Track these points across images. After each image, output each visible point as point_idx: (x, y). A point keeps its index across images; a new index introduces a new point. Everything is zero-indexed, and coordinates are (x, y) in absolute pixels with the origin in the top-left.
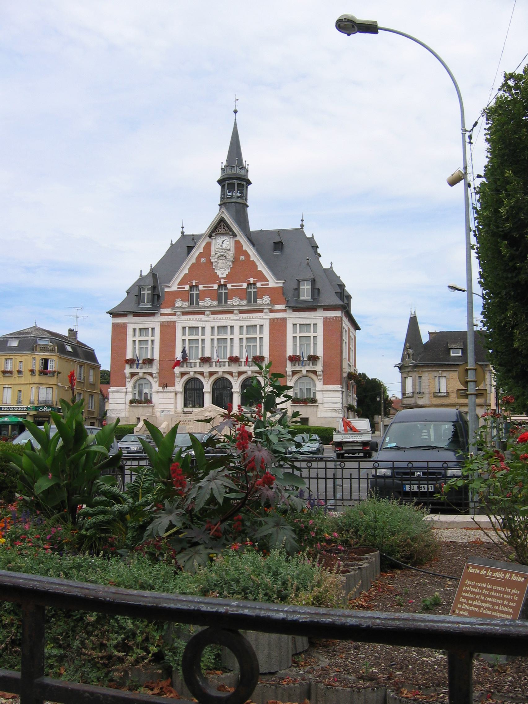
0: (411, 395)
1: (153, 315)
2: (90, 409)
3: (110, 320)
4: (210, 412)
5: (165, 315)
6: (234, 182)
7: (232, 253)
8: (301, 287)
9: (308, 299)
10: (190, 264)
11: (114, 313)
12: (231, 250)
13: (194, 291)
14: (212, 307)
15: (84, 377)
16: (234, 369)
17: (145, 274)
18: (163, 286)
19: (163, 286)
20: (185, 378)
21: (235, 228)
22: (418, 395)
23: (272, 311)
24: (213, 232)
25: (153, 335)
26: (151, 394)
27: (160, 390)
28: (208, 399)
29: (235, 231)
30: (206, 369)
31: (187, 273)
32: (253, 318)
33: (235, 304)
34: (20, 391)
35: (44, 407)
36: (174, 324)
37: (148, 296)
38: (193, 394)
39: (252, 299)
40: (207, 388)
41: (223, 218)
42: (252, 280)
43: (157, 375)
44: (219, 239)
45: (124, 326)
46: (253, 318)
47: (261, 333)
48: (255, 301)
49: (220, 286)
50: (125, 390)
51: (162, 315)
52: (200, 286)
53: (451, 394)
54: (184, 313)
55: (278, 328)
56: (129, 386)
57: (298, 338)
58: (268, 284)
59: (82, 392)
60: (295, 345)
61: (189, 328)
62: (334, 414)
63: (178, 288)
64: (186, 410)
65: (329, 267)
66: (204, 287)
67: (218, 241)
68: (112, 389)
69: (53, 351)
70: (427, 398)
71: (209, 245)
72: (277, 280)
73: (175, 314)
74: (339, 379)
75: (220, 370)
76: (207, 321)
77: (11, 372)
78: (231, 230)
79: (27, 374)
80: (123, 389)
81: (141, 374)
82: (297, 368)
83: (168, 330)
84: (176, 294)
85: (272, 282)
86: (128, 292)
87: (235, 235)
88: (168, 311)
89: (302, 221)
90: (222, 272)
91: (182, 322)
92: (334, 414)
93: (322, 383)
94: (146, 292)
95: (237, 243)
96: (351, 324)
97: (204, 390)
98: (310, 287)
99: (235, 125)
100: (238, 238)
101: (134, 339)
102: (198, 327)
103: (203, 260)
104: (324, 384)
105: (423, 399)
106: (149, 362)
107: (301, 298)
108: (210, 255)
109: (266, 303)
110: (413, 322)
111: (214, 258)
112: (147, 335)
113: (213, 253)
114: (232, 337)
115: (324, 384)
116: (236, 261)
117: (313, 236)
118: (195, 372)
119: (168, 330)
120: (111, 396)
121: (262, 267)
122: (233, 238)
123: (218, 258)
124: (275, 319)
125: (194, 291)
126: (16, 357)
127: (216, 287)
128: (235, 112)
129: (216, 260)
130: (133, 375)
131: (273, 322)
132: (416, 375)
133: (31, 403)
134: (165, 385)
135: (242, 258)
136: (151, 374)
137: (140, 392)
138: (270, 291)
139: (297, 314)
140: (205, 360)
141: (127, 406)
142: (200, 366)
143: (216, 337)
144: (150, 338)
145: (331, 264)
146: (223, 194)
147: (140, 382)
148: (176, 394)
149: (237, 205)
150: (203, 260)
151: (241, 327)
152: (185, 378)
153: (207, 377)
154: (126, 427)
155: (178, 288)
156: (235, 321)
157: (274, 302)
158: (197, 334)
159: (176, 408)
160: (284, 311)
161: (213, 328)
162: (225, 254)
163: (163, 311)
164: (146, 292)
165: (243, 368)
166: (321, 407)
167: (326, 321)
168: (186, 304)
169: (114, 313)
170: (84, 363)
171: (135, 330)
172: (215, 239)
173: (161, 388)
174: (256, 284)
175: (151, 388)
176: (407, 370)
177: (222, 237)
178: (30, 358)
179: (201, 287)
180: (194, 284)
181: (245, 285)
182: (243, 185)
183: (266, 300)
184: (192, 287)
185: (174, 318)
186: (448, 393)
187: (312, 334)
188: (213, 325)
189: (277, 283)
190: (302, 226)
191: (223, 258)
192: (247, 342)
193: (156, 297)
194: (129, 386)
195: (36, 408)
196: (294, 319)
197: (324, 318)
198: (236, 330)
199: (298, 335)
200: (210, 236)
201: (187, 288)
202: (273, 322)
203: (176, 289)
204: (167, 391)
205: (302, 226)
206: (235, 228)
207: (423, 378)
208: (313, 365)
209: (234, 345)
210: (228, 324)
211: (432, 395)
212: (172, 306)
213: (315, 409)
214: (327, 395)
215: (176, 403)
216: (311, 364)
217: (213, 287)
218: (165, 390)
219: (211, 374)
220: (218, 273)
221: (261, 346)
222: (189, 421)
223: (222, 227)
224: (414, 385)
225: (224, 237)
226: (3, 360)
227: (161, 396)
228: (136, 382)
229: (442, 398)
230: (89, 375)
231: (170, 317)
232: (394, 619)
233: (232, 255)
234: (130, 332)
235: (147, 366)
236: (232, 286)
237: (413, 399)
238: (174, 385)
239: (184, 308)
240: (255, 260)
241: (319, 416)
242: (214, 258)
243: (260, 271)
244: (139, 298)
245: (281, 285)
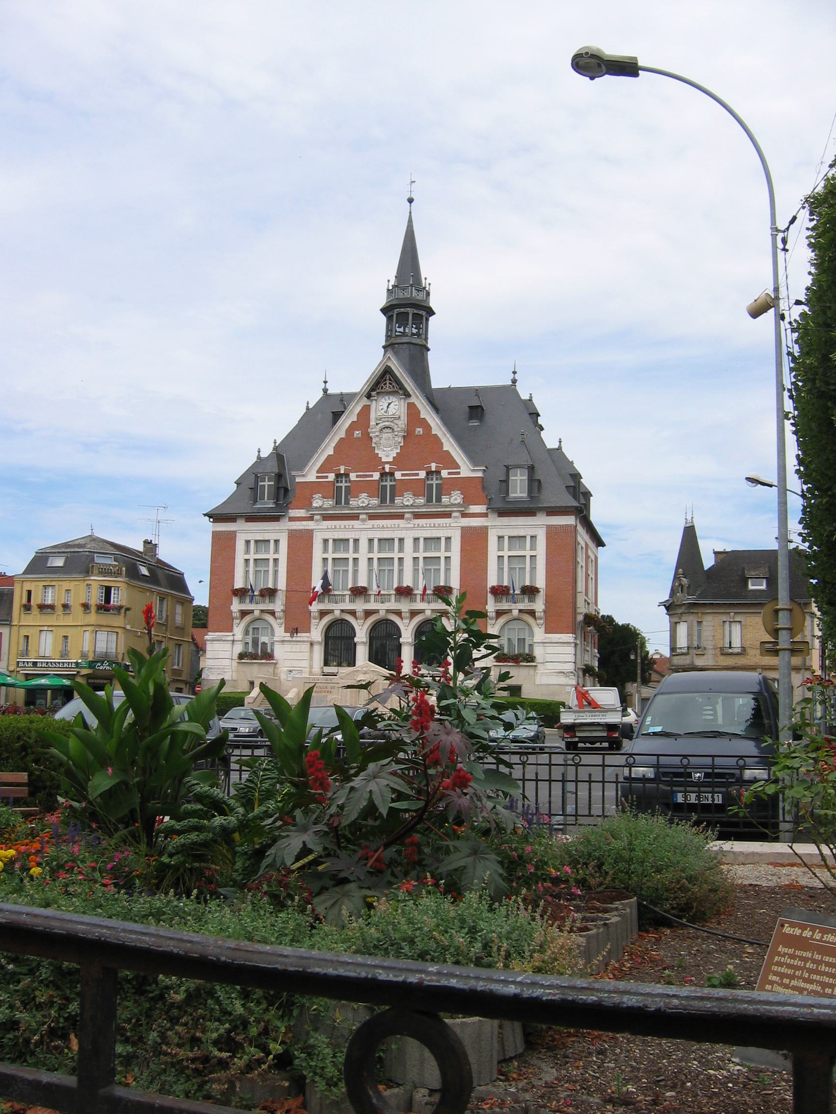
0: (685, 651)
1: (277, 519)
2: (176, 667)
3: (209, 527)
4: (365, 673)
5: (298, 519)
6: (408, 311)
7: (402, 423)
8: (512, 478)
9: (522, 497)
10: (336, 439)
11: (216, 516)
12: (402, 418)
13: (341, 482)
14: (370, 508)
15: (167, 616)
16: (405, 606)
17: (265, 454)
18: (293, 473)
19: (293, 473)
20: (327, 619)
21: (409, 384)
22: (695, 651)
23: (464, 515)
24: (373, 389)
25: (276, 551)
26: (272, 644)
27: (286, 639)
28: (362, 653)
29: (409, 389)
30: (360, 606)
32: (434, 526)
34: (66, 637)
35: (103, 662)
36: (309, 533)
37: (270, 489)
38: (338, 646)
39: (433, 497)
40: (361, 635)
41: (389, 367)
42: (433, 467)
43: (281, 614)
44: (383, 400)
45: (231, 537)
46: (434, 526)
47: (448, 549)
48: (439, 500)
49: (383, 474)
50: (231, 638)
51: (292, 519)
52: (351, 475)
53: (748, 650)
54: (326, 518)
55: (474, 542)
56: (238, 631)
57: (506, 559)
58: (459, 473)
59: (163, 639)
60: (500, 569)
61: (334, 540)
62: (562, 680)
63: (318, 477)
64: (327, 669)
65: (555, 445)
66: (357, 476)
67: (381, 404)
68: (210, 636)
69: (118, 574)
70: (710, 657)
71: (366, 410)
72: (475, 466)
73: (311, 518)
74: (570, 625)
75: (382, 607)
76: (362, 530)
77: (52, 607)
78: (401, 387)
79: (77, 609)
80: (228, 636)
81: (257, 613)
82: (505, 606)
83: (300, 544)
84: (314, 487)
85: (466, 470)
86: (238, 483)
87: (408, 395)
88: (301, 513)
89: (514, 373)
90: (387, 453)
91: (323, 531)
92: (562, 680)
93: (543, 629)
94: (266, 483)
95: (412, 407)
96: (591, 538)
97: (356, 640)
98: (526, 478)
99: (410, 221)
100: (413, 400)
101: (247, 557)
102: (348, 540)
103: (357, 434)
104: (547, 632)
105: (704, 657)
106: (270, 593)
107: (512, 495)
109: (456, 502)
110: (690, 536)
111: (374, 431)
112: (267, 551)
113: (373, 423)
114: (401, 555)
115: (547, 632)
116: (408, 435)
117: (531, 397)
118: (342, 611)
119: (300, 544)
120: (209, 647)
121: (449, 445)
122: (405, 399)
124: (470, 528)
125: (341, 482)
126: (60, 583)
127: (376, 476)
128: (411, 201)
129: (377, 434)
130: (244, 613)
132: (693, 619)
133: (84, 655)
134: (294, 631)
135: (419, 431)
136: (272, 613)
137: (255, 642)
138: (463, 484)
139: (505, 520)
140: (359, 592)
141: (235, 663)
142: (350, 601)
143: (376, 555)
144: (271, 556)
145: (560, 442)
146: (389, 329)
147: (256, 625)
148: (312, 644)
149: (412, 347)
150: (357, 434)
151: (416, 540)
152: (327, 619)
153: (360, 619)
154: (233, 695)
155: (318, 477)
156: (406, 530)
157: (468, 500)
158: (347, 550)
159: (311, 667)
160: (485, 515)
161: (371, 541)
163: (293, 513)
164: (266, 483)
165: (419, 605)
166: (541, 669)
167: (552, 533)
168: (330, 503)
169: (216, 516)
170: (168, 594)
171: (248, 542)
172: (376, 400)
173: (288, 634)
174: (440, 472)
175: (273, 634)
176: (679, 611)
177: (387, 398)
178: (82, 586)
179: (353, 476)
180: (342, 472)
181: (422, 474)
182: (422, 316)
183: (457, 497)
184: (338, 476)
185: (310, 525)
186: (743, 648)
187: (528, 553)
188: (371, 537)
189: (473, 470)
190: (514, 381)
192: (425, 564)
193: (282, 491)
194: (238, 631)
195: (92, 664)
196: (499, 528)
197: (549, 527)
198: (409, 544)
199: (506, 553)
201: (331, 477)
203: (314, 480)
204: (298, 639)
205: (514, 381)
206: (409, 384)
207: (704, 623)
208: (530, 601)
209: (405, 568)
210: (396, 535)
211: (718, 652)
212: (308, 506)
213: (531, 671)
214: (550, 649)
215: (311, 659)
216: (526, 600)
217: (372, 476)
218: (294, 639)
219: (368, 613)
220: (381, 454)
221: (447, 570)
222: (332, 687)
223: (388, 382)
224: (690, 635)
225: (391, 397)
226: (41, 587)
227: (287, 647)
228: (248, 626)
229: (734, 657)
230: (174, 614)
231: (304, 523)
232: (701, 998)
233: (403, 426)
234: (240, 546)
235: (267, 600)
236: (403, 475)
237: (688, 657)
238: (309, 631)
239: (326, 509)
240: (440, 434)
241: (538, 682)
242: (374, 430)
243: (447, 452)
244: (255, 492)
245: (480, 474)
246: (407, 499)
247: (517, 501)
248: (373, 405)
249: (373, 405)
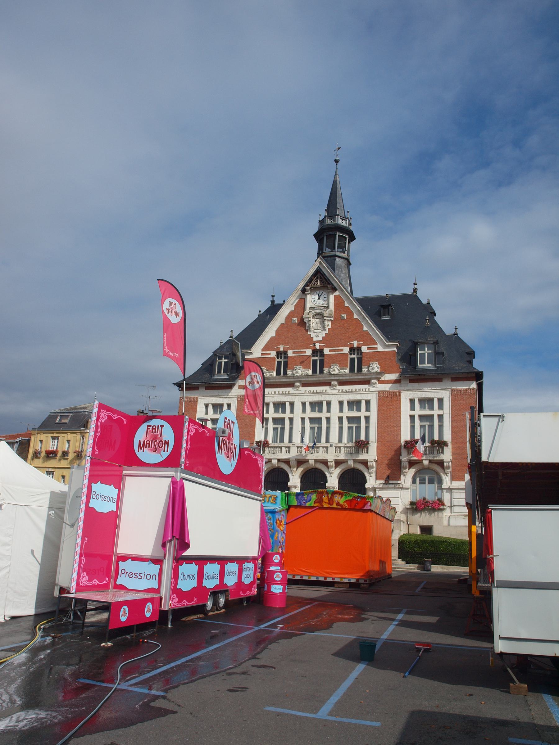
9: (429, 367)
31: (274, 335)
33: (333, 373)
49: (315, 352)
55: (389, 404)
58: (376, 348)
63: (262, 354)
66: (294, 353)
71: (302, 301)
72: (390, 342)
78: (329, 283)
104: (453, 479)
109: (374, 371)
115: (453, 479)
126: (63, 435)
127: (309, 352)
131: (382, 396)
155: (262, 354)
156: (334, 395)
161: (304, 404)
164: (223, 360)
179: (290, 353)
181: (346, 350)
191: (321, 317)
201: (273, 354)
202: (382, 396)
217: (305, 352)
220: (312, 335)
236: (330, 351)
242: (308, 316)
246: (336, 370)
247: (424, 371)
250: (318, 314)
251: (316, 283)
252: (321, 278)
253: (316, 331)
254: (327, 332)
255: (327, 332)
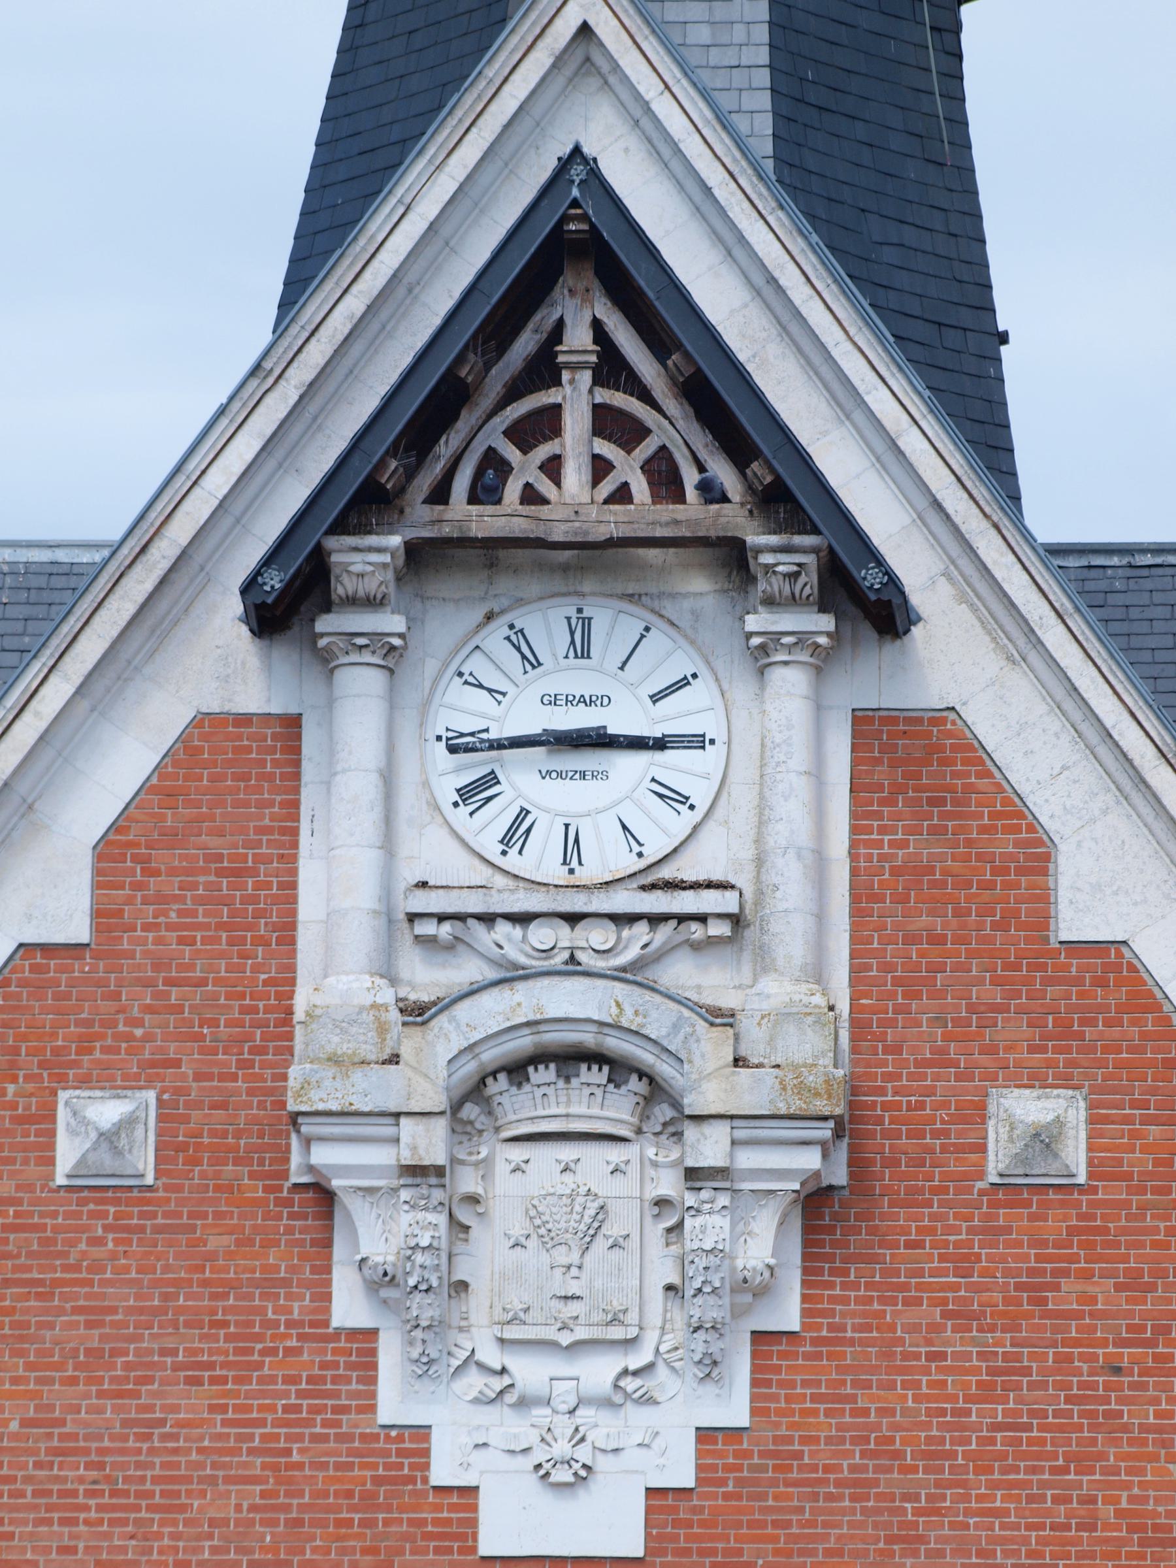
7: (790, 1000)
12: (788, 928)
24: (359, 497)
71: (240, 782)
87: (868, 605)
95: (914, 771)
108: (277, 1027)
122: (824, 661)
123: (470, 1102)
162: (659, 1019)
172: (391, 655)
177: (547, 626)
191: (616, 1108)
200: (291, 601)
223: (576, 398)
242: (371, 1089)
248: (354, 724)
249: (354, 724)
250: (570, 1059)
251: (526, 469)
252: (611, 367)
253: (530, 1372)
254: (734, 1409)
255: (734, 1409)
